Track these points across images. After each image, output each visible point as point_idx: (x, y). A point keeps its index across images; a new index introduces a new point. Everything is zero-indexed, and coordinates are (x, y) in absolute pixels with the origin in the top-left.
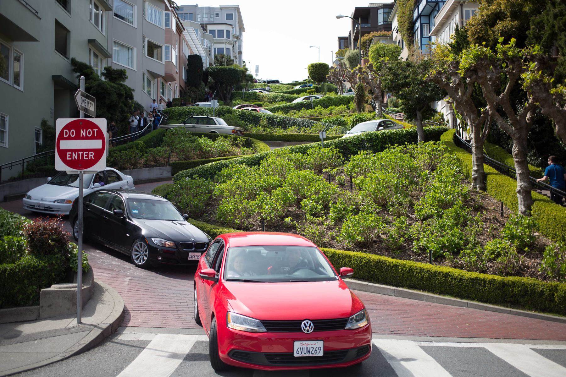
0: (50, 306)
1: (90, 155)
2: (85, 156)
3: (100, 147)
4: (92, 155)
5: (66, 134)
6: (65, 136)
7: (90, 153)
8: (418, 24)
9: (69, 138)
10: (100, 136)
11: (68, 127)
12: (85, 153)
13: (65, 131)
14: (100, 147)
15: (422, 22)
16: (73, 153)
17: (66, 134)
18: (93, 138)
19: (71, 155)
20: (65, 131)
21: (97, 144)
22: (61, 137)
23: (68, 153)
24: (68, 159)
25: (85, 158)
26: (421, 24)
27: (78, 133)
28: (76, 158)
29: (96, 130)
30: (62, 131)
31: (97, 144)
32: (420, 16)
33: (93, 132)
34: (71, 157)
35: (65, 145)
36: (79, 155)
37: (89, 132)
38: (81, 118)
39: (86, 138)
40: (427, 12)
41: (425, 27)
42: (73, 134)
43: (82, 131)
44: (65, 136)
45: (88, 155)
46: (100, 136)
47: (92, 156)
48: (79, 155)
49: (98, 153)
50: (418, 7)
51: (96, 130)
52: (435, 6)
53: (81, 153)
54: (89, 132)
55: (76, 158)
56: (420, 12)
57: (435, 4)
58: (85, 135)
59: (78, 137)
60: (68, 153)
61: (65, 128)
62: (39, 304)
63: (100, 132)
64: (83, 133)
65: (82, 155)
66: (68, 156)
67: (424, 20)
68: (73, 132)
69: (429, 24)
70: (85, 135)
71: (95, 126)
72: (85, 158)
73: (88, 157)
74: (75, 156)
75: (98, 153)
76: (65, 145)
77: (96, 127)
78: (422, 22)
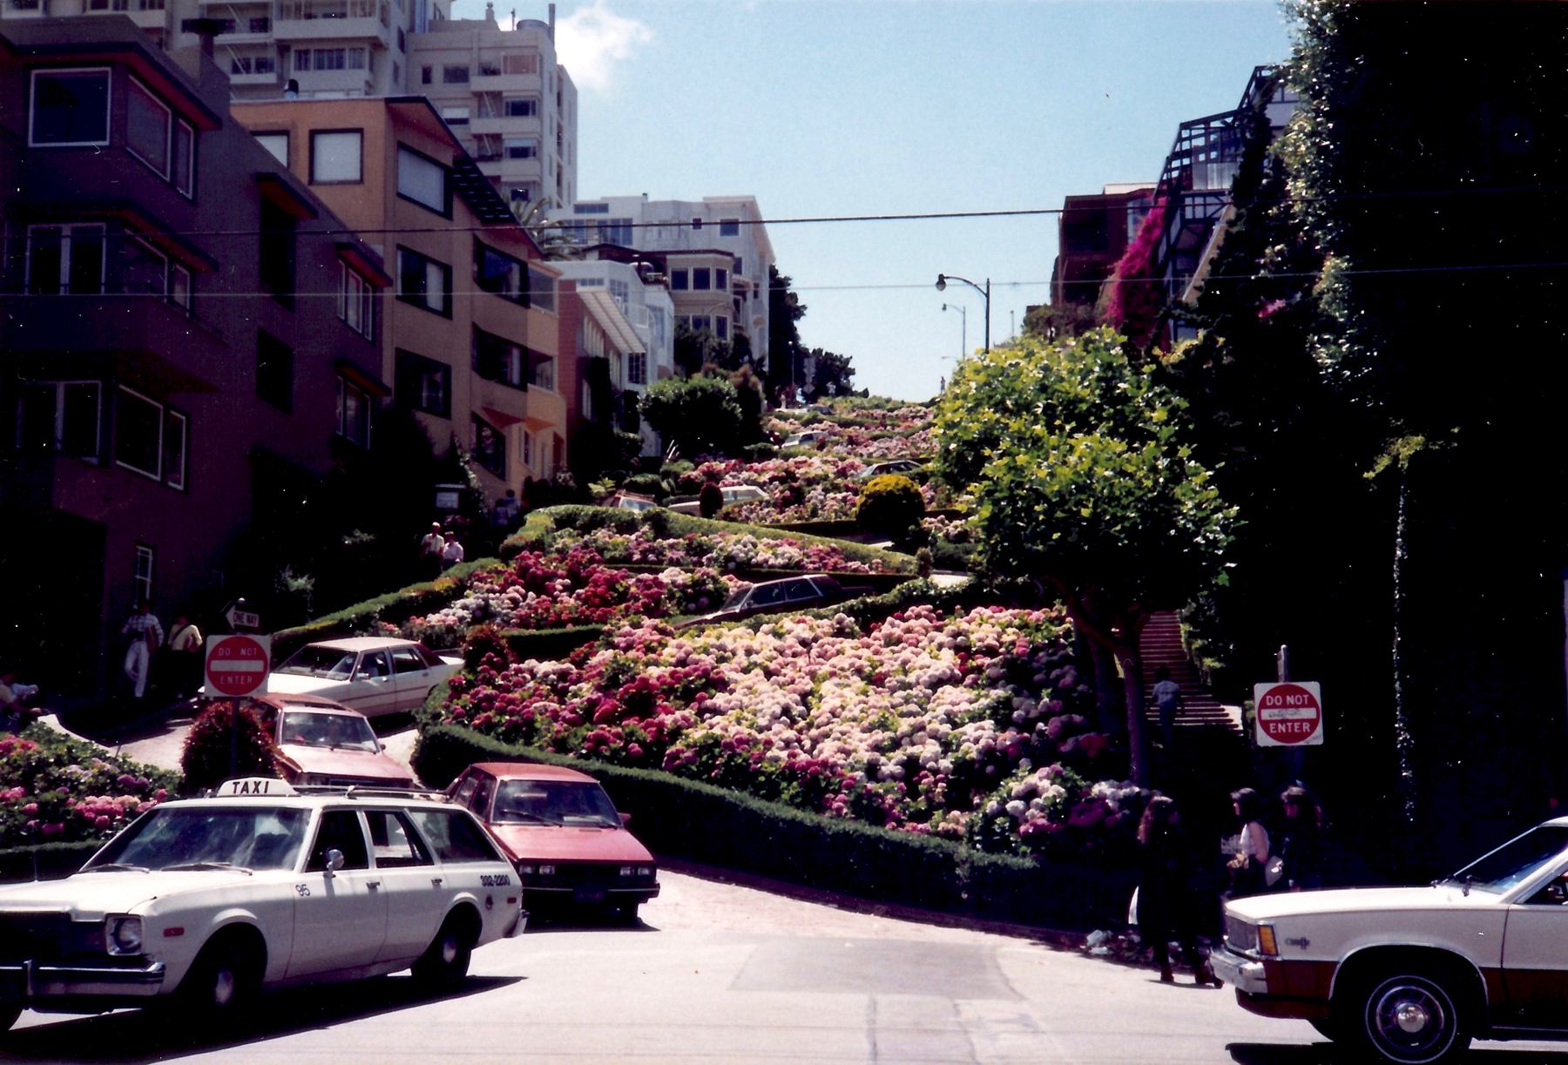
4: (1306, 727)
6: (1268, 704)
9: (1274, 706)
10: (1311, 703)
11: (1272, 693)
12: (1296, 724)
13: (1268, 697)
16: (1280, 725)
18: (1303, 706)
20: (1268, 697)
21: (1310, 713)
22: (1263, 705)
27: (1284, 700)
29: (1306, 696)
31: (1310, 713)
36: (1287, 727)
44: (1268, 704)
46: (1311, 703)
48: (1287, 727)
51: (1306, 696)
53: (1289, 724)
54: (1299, 699)
59: (1285, 706)
61: (1269, 693)
63: (1311, 698)
64: (1290, 700)
65: (1293, 727)
71: (1303, 691)
74: (1282, 728)
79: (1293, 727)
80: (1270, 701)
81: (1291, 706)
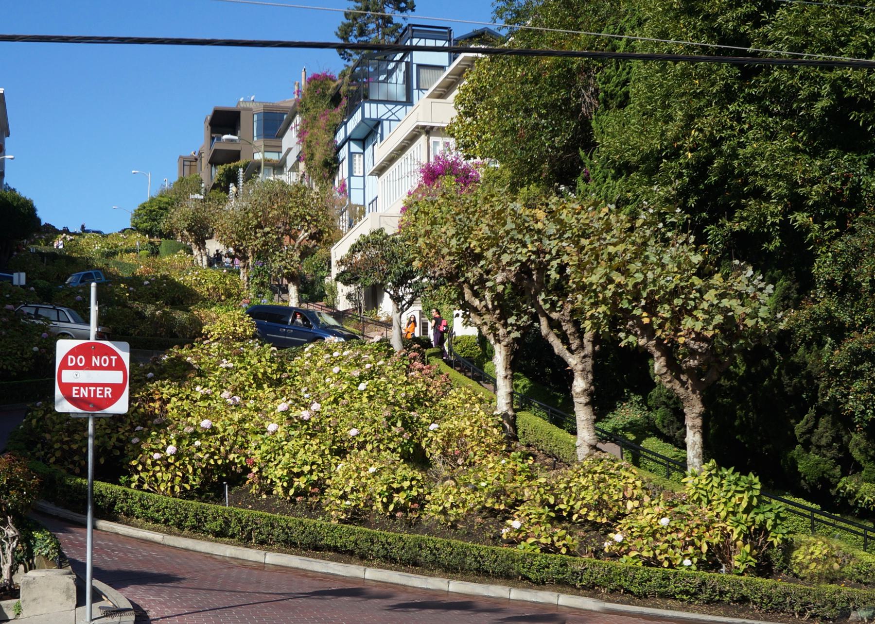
0: (34, 600)
1: (106, 392)
2: (98, 392)
3: (121, 382)
4: (108, 392)
5: (72, 361)
6: (70, 364)
7: (106, 389)
8: (344, 153)
9: (76, 367)
10: (120, 366)
11: (74, 352)
12: (98, 388)
13: (70, 357)
14: (121, 382)
15: (352, 151)
17: (72, 361)
18: (110, 368)
19: (79, 391)
20: (70, 357)
21: (116, 377)
22: (64, 365)
23: (74, 388)
24: (74, 396)
25: (98, 396)
26: (351, 155)
28: (86, 395)
29: (114, 358)
30: (65, 358)
31: (116, 377)
32: (348, 139)
33: (111, 360)
34: (79, 393)
35: (68, 376)
36: (89, 391)
37: (105, 361)
38: (92, 339)
39: (101, 368)
40: (360, 135)
41: (358, 160)
42: (81, 361)
43: (94, 358)
44: (70, 364)
45: (103, 391)
46: (120, 366)
47: (109, 393)
48: (89, 391)
49: (117, 390)
50: (346, 124)
51: (114, 358)
52: (376, 126)
53: (92, 389)
54: (105, 361)
55: (86, 395)
56: (348, 134)
57: (376, 123)
58: (98, 364)
59: (89, 366)
60: (74, 388)
61: (71, 353)
62: (19, 597)
63: (119, 360)
64: (95, 361)
65: (95, 391)
66: (74, 392)
67: (355, 148)
68: (81, 361)
69: (363, 153)
70: (98, 364)
71: (110, 352)
72: (98, 396)
73: (103, 394)
74: (84, 393)
75: (117, 390)
76: (68, 376)
77: (115, 353)
78: (352, 151)
79: (95, 391)
80: (72, 361)
81: (96, 368)
